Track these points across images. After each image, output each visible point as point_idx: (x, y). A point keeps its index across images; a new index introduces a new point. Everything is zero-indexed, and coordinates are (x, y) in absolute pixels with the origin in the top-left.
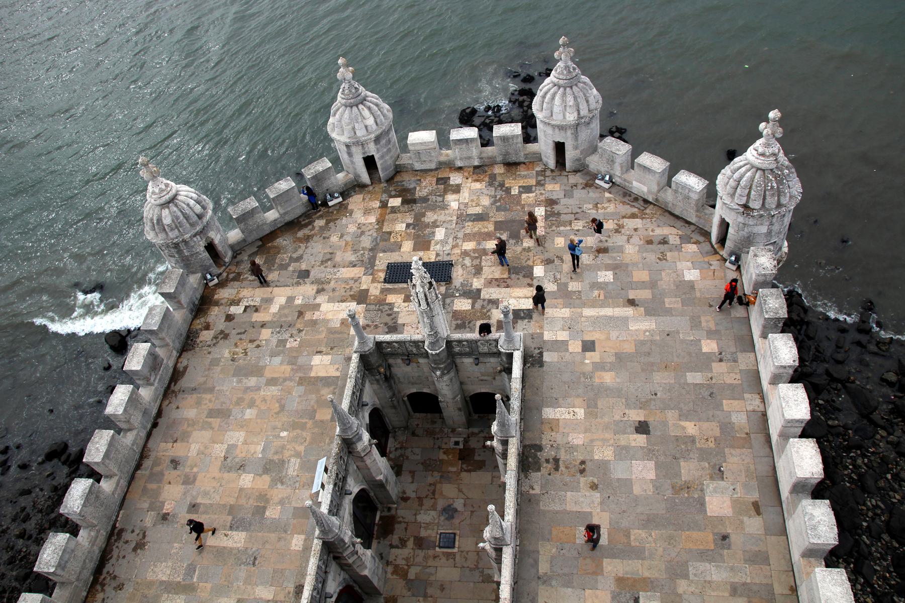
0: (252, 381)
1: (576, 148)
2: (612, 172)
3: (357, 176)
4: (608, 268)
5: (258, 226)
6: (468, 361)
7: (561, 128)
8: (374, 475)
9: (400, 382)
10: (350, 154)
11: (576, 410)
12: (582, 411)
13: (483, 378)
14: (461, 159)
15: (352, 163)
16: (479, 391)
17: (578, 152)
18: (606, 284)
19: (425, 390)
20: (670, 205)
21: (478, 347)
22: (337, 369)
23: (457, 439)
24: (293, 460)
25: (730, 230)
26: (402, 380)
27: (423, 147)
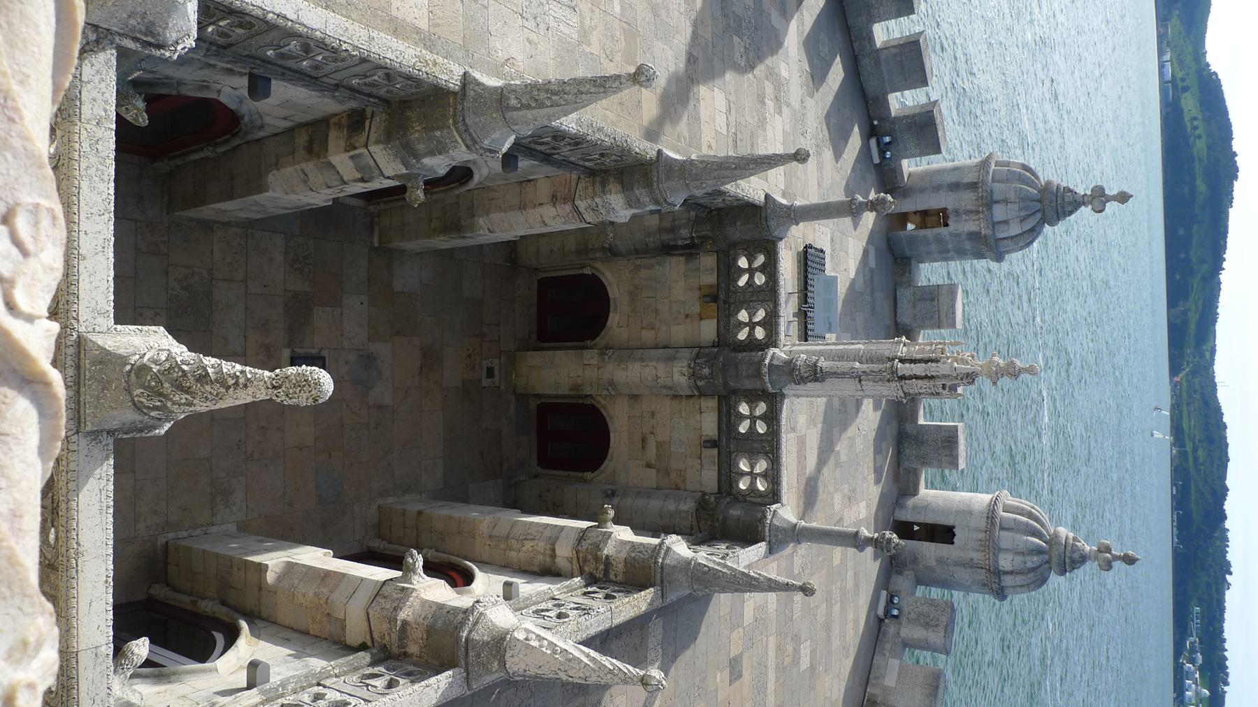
1: (941, 561)
2: (904, 620)
4: (813, 652)
6: (709, 425)
8: (496, 217)
9: (637, 268)
10: (955, 187)
13: (651, 445)
17: (933, 563)
19: (613, 319)
21: (752, 456)
22: (710, 147)
23: (496, 372)
24: (575, 20)
26: (644, 273)
27: (944, 309)
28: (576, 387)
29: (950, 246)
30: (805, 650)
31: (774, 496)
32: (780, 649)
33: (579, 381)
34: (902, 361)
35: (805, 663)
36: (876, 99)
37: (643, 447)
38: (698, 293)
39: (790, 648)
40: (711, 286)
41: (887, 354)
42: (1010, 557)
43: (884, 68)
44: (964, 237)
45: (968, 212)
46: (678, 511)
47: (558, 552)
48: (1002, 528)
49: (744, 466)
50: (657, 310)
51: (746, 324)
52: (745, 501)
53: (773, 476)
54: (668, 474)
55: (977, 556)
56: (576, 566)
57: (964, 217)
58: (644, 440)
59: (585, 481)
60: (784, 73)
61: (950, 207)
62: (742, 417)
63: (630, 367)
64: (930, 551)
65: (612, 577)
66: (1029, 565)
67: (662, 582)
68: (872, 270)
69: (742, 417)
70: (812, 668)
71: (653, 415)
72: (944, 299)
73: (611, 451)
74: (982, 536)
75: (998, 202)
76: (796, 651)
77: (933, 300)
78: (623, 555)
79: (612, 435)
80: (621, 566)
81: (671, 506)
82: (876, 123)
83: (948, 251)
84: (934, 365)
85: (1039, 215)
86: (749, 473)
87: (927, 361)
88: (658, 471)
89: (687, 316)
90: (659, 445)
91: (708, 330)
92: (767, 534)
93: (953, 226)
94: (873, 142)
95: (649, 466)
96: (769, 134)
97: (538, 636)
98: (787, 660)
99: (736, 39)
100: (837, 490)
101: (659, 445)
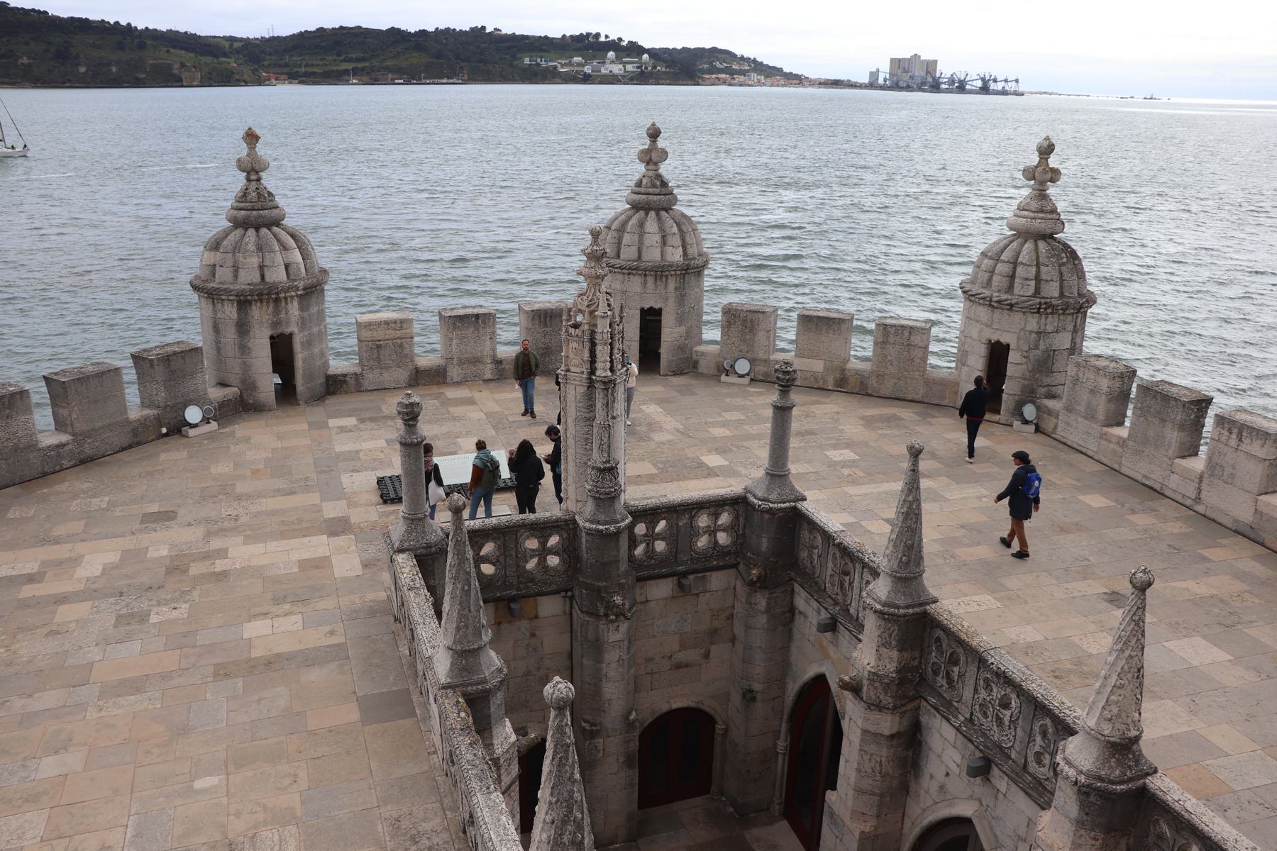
0: (50, 699)
1: (680, 320)
3: (249, 385)
4: (835, 447)
5: (16, 449)
6: (661, 590)
7: (660, 272)
10: (243, 328)
11: (976, 598)
12: (988, 597)
13: (683, 656)
14: (461, 362)
15: (244, 349)
16: (665, 708)
17: (682, 329)
18: (854, 461)
20: (873, 382)
21: (694, 533)
22: (332, 633)
25: (1013, 357)
27: (392, 333)
28: (629, 763)
29: (315, 330)
30: (837, 455)
31: (738, 503)
32: (854, 482)
33: (622, 759)
34: (593, 371)
35: (848, 454)
36: (135, 432)
37: (687, 666)
38: (504, 626)
39: (846, 471)
40: (497, 610)
41: (582, 390)
42: (669, 249)
43: (98, 425)
44: (306, 314)
45: (277, 311)
46: (768, 611)
47: (894, 731)
48: (640, 257)
49: (702, 542)
50: (528, 673)
51: (542, 560)
52: (743, 535)
53: (715, 505)
54: (716, 630)
55: (672, 284)
56: (910, 706)
57: (283, 315)
58: (679, 666)
59: (726, 730)
60: (164, 552)
61: (269, 333)
62: (650, 551)
63: (608, 696)
64: (670, 333)
65: (916, 663)
66: (675, 229)
67: (921, 605)
68: (362, 421)
69: (650, 551)
70: (848, 446)
71: (649, 660)
72: (380, 334)
73: (692, 704)
74: (650, 280)
75: (263, 277)
76: (845, 464)
77: (379, 347)
78: (895, 654)
79: (674, 706)
80: (906, 655)
81: (762, 620)
82: (164, 430)
83: (320, 331)
84: (598, 337)
85: (275, 229)
86: (714, 534)
87: (593, 345)
88: (712, 643)
89: (533, 635)
90: (683, 647)
91: (550, 607)
92: (787, 505)
93: (293, 328)
94: (192, 432)
95: (707, 656)
96: (263, 561)
97: (1104, 708)
98: (860, 473)
99: (154, 619)
100: (650, 439)
101: (683, 647)
